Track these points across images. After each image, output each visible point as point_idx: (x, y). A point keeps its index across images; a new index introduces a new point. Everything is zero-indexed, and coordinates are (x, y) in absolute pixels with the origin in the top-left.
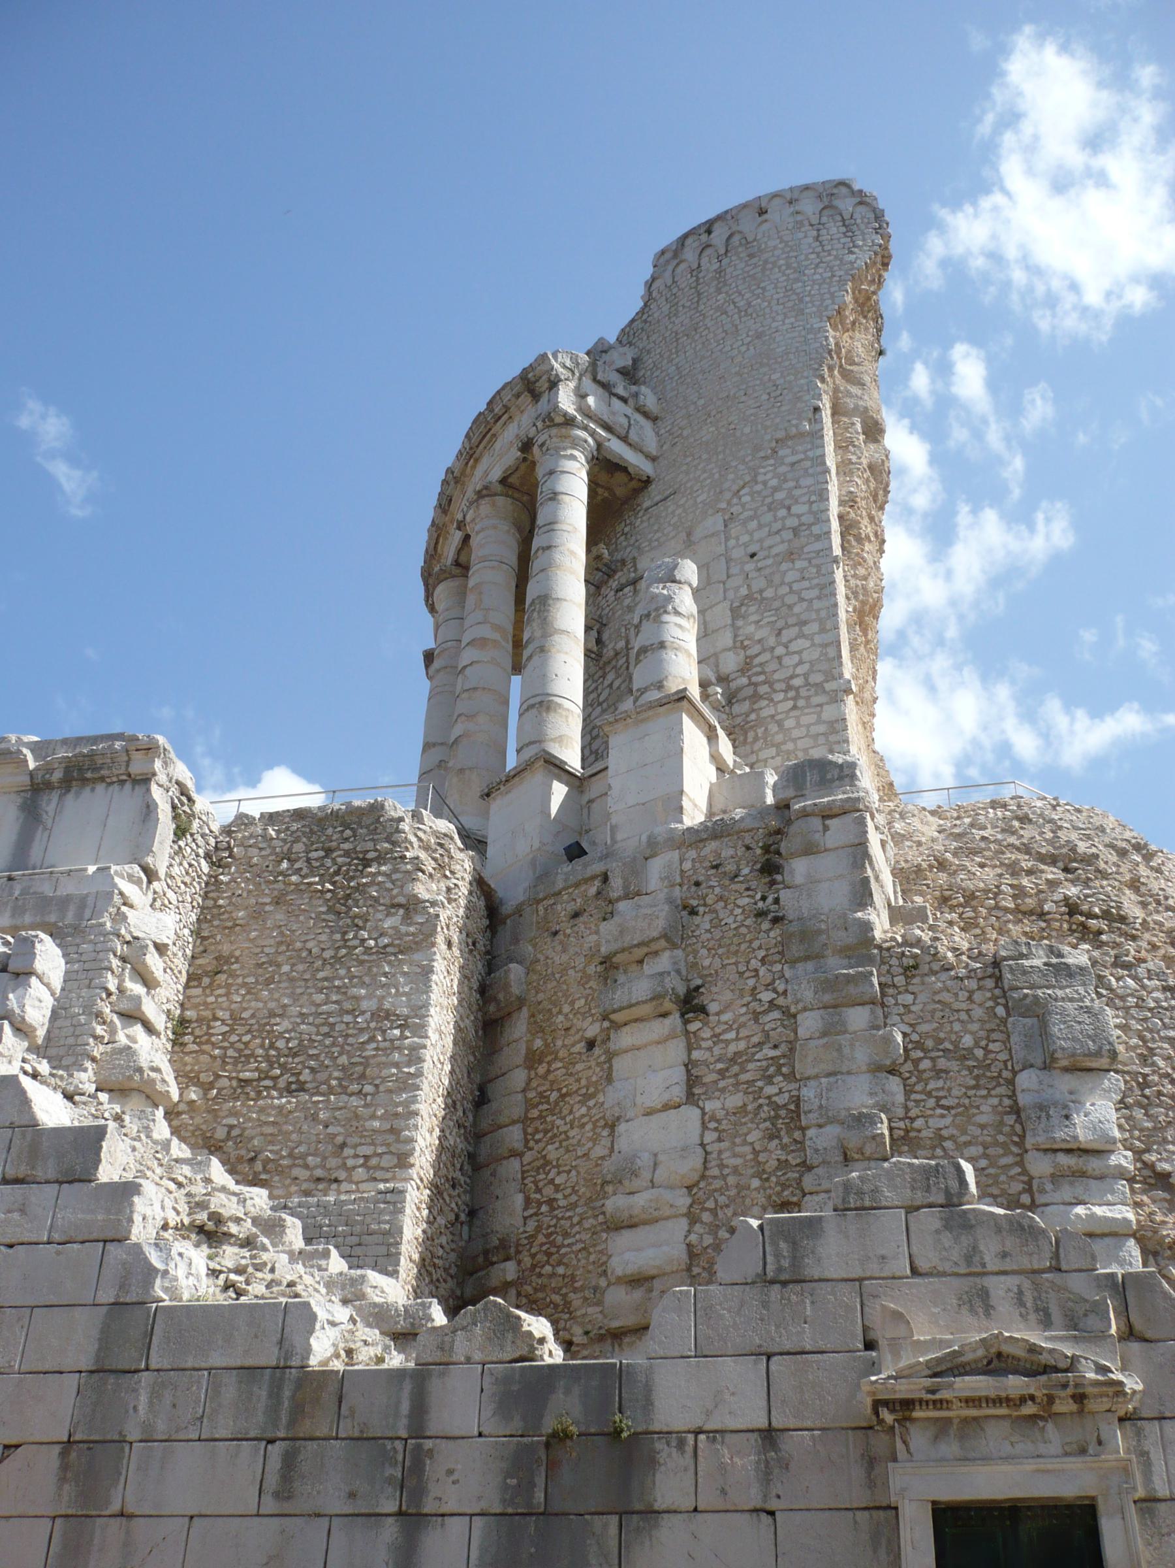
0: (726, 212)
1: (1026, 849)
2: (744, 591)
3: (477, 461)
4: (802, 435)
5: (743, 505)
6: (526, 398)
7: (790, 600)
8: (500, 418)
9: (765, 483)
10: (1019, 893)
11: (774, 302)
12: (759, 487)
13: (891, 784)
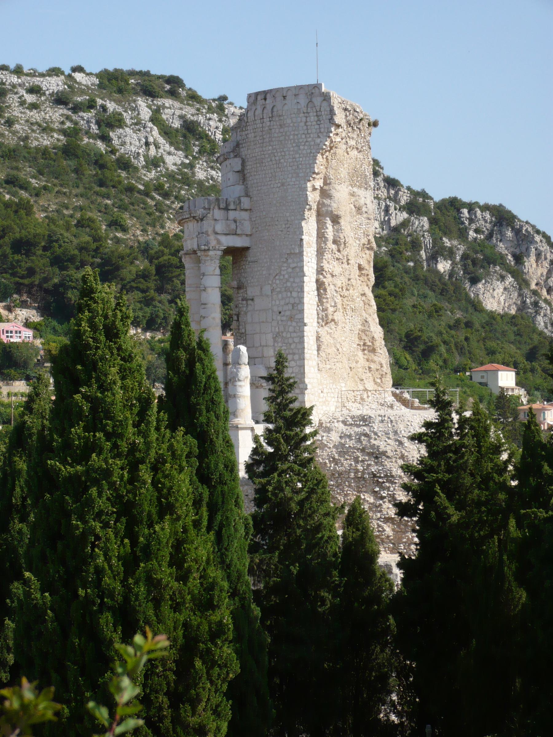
0: (271, 90)
1: (363, 450)
2: (277, 330)
4: (295, 254)
5: (277, 284)
7: (290, 341)
9: (284, 276)
10: (357, 471)
12: (282, 277)
13: (373, 337)
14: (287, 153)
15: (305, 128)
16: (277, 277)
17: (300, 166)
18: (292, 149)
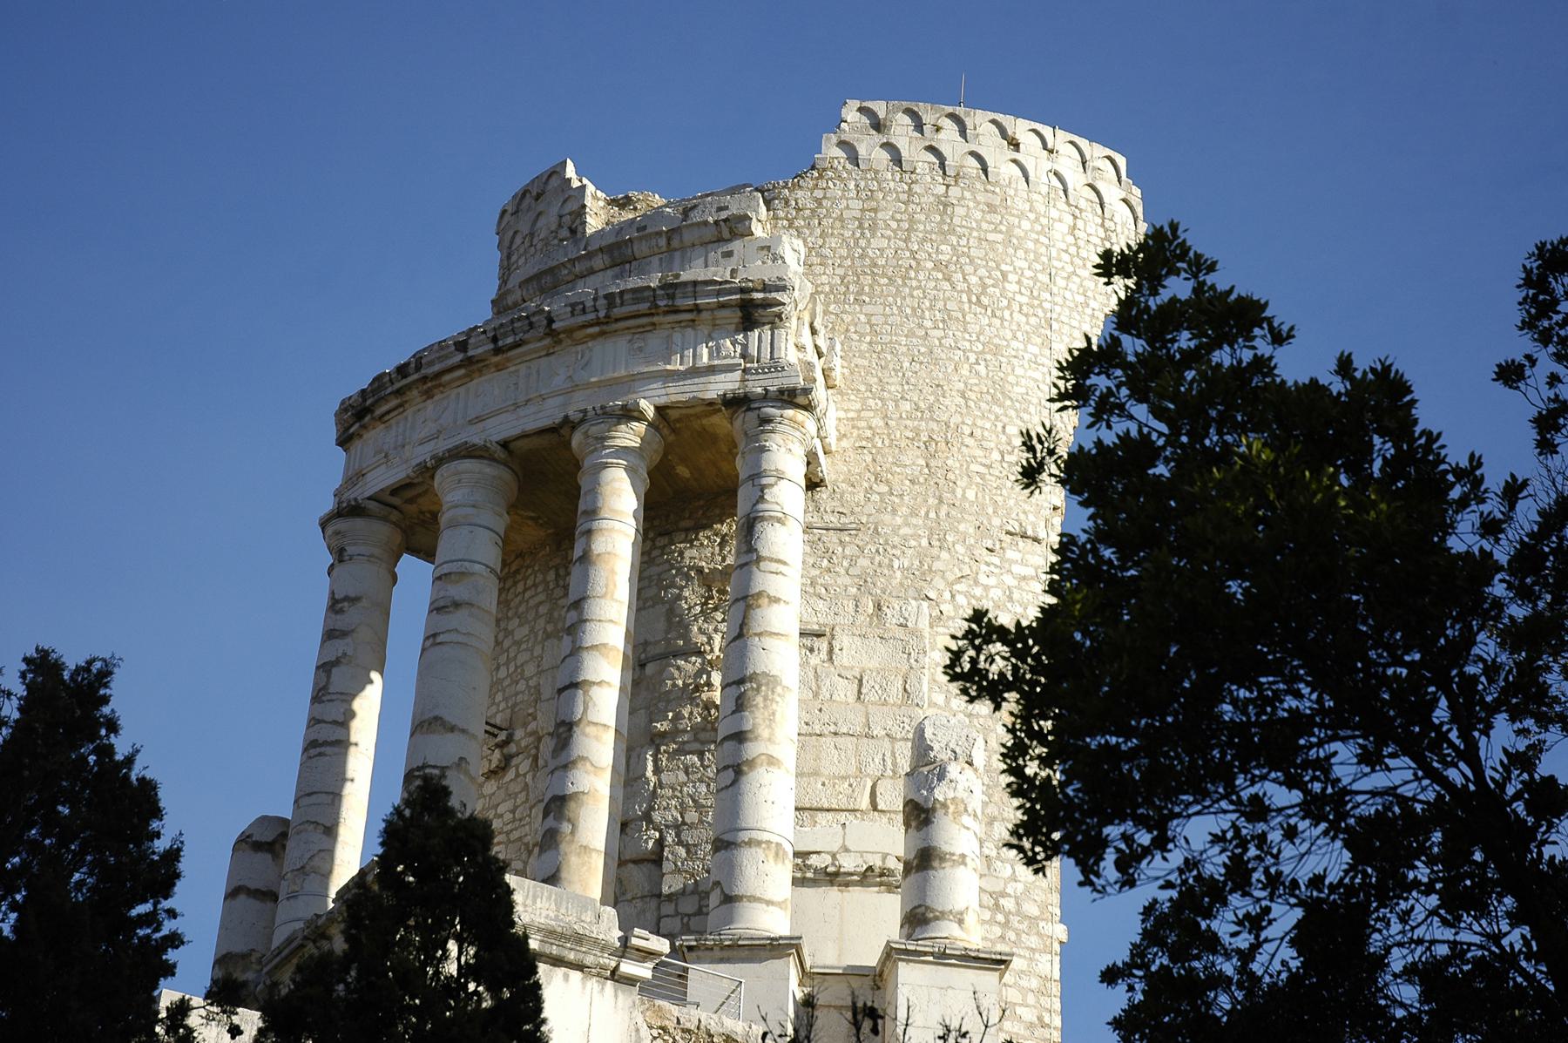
3: (602, 333)
8: (677, 311)
11: (1016, 307)
14: (1012, 277)
15: (1071, 239)
16: (957, 587)
17: (1055, 326)
18: (1028, 273)
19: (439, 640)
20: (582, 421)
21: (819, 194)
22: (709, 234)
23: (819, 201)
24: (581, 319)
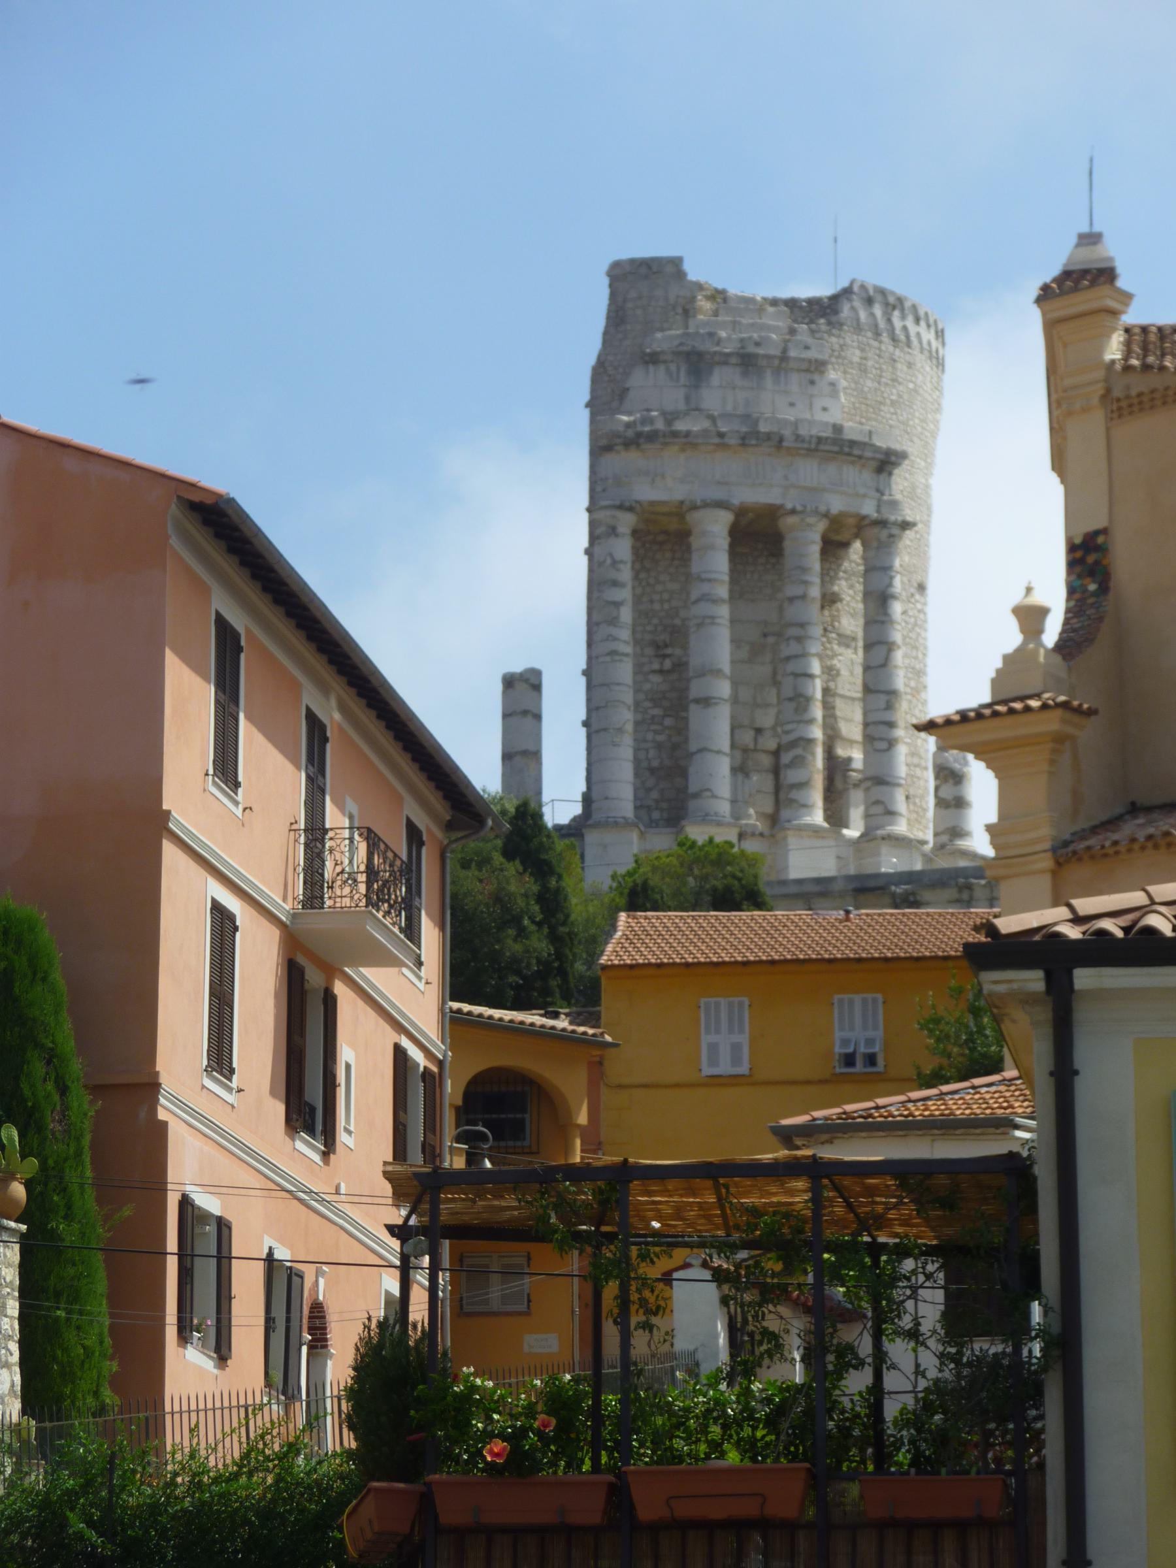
6: (874, 464)
8: (849, 454)
19: (718, 621)
20: (802, 512)
21: (841, 342)
22: (804, 366)
23: (841, 346)
24: (800, 445)
